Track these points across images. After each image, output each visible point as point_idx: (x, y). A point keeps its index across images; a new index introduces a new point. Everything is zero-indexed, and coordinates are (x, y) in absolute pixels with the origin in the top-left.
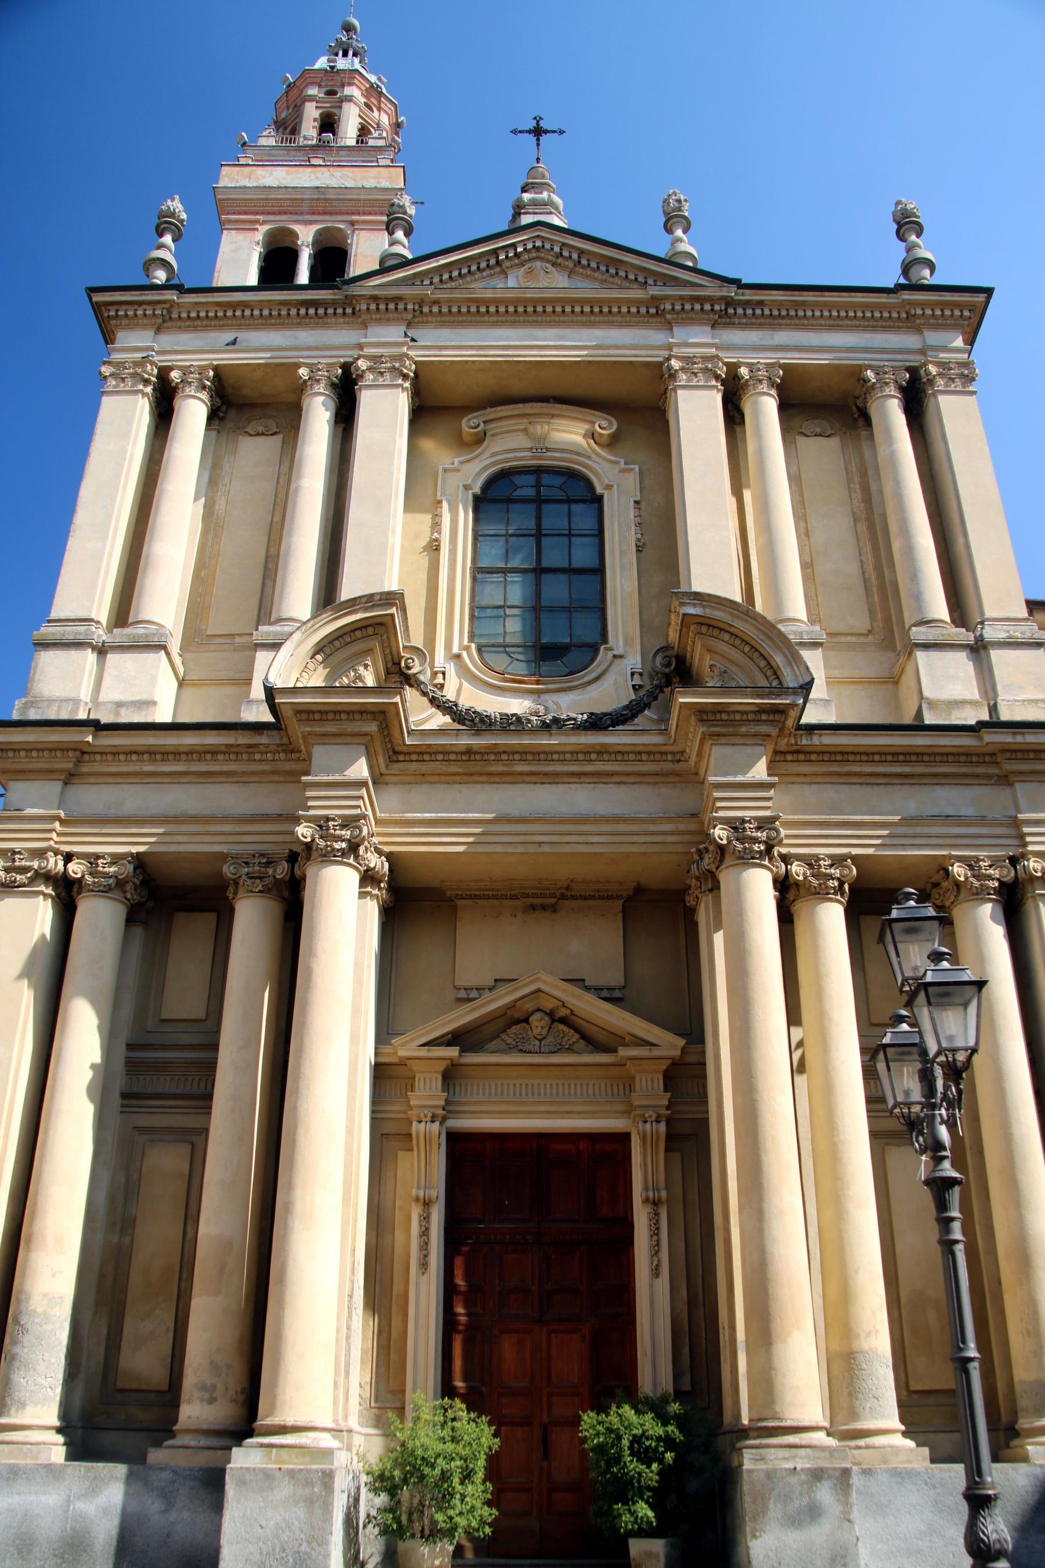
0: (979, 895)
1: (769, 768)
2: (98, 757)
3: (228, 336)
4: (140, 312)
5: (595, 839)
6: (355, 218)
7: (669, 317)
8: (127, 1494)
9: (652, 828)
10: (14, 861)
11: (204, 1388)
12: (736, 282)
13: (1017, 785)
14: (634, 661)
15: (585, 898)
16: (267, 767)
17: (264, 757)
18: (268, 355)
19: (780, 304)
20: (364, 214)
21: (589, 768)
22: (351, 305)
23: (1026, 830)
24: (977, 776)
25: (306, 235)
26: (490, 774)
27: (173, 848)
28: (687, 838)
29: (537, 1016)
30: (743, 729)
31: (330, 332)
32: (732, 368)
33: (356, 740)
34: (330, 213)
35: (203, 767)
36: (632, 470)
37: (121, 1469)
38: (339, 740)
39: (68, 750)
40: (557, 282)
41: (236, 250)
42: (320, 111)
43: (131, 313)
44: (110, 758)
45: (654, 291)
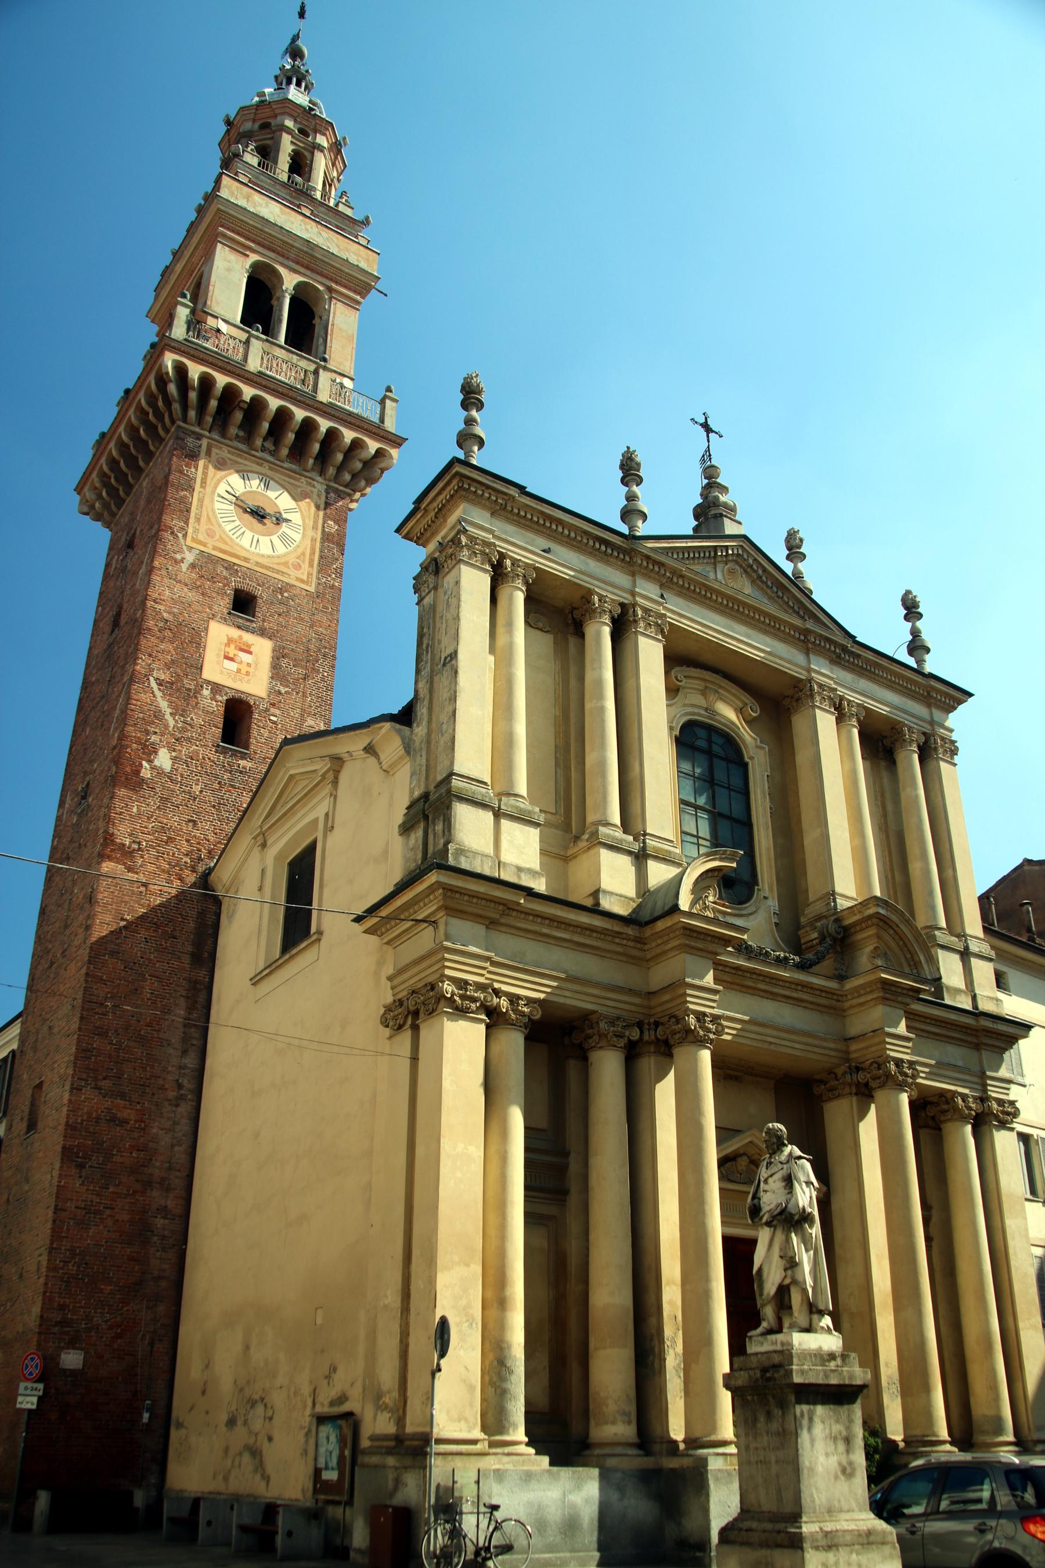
0: (964, 1119)
1: (907, 1026)
2: (514, 913)
3: (545, 543)
4: (487, 495)
5: (797, 1046)
6: (334, 285)
7: (810, 646)
8: (601, 1489)
9: (825, 1044)
10: (466, 990)
11: (624, 1414)
12: (853, 637)
13: (983, 1052)
14: (773, 904)
15: (756, 1075)
16: (620, 949)
17: (621, 942)
18: (572, 573)
19: (868, 660)
20: (345, 287)
21: (795, 995)
22: (629, 554)
23: (989, 1082)
24: (966, 1041)
25: (290, 281)
26: (743, 986)
27: (562, 1000)
28: (833, 1053)
29: (745, 1158)
30: (900, 999)
31: (610, 569)
32: (842, 698)
33: (709, 956)
34: (312, 270)
35: (582, 940)
36: (764, 748)
37: (595, 1472)
38: (699, 953)
39: (529, 914)
40: (745, 589)
41: (229, 270)
42: (293, 147)
43: (480, 492)
44: (523, 916)
45: (810, 625)
